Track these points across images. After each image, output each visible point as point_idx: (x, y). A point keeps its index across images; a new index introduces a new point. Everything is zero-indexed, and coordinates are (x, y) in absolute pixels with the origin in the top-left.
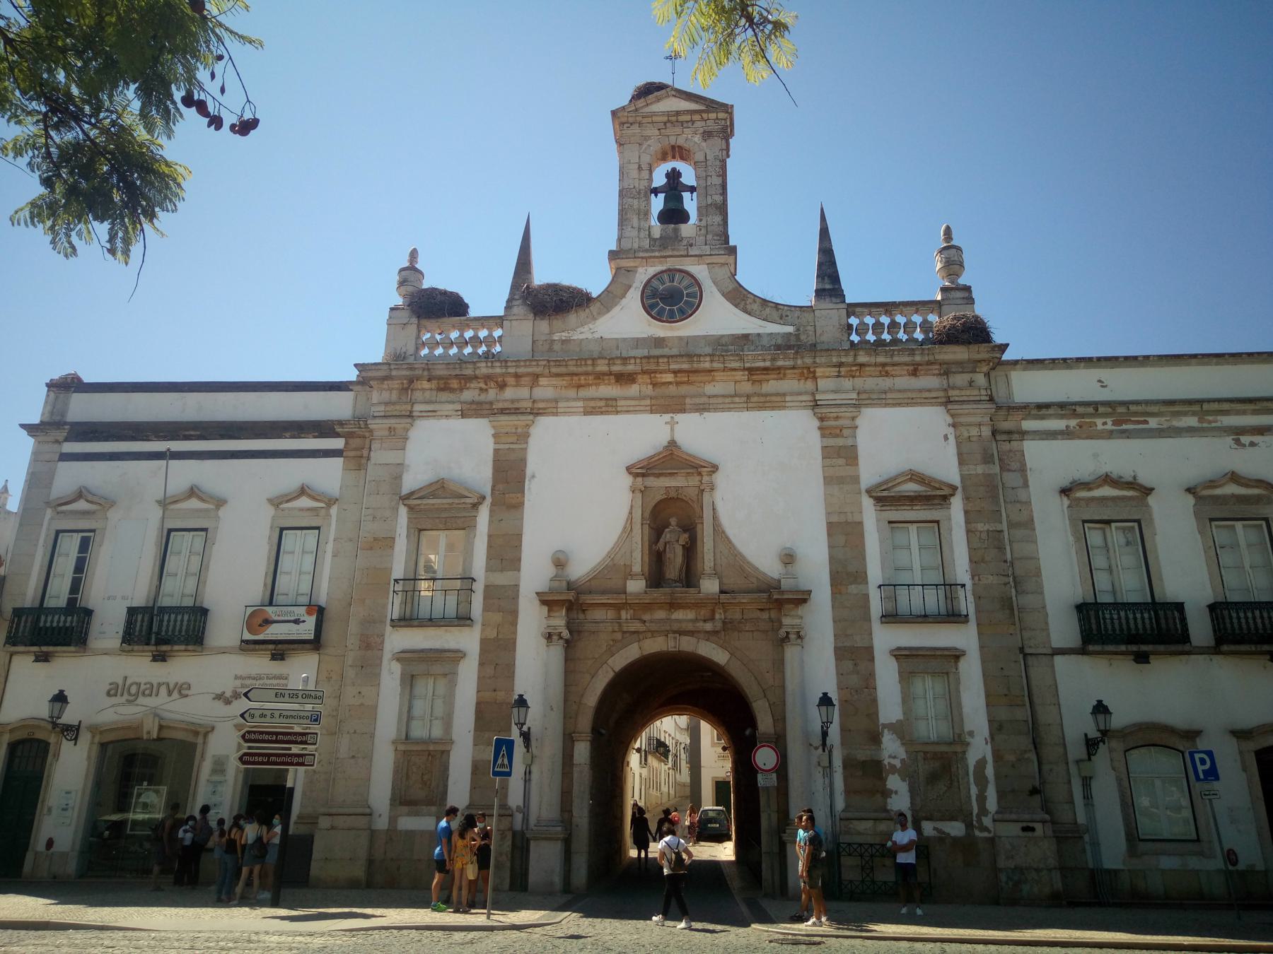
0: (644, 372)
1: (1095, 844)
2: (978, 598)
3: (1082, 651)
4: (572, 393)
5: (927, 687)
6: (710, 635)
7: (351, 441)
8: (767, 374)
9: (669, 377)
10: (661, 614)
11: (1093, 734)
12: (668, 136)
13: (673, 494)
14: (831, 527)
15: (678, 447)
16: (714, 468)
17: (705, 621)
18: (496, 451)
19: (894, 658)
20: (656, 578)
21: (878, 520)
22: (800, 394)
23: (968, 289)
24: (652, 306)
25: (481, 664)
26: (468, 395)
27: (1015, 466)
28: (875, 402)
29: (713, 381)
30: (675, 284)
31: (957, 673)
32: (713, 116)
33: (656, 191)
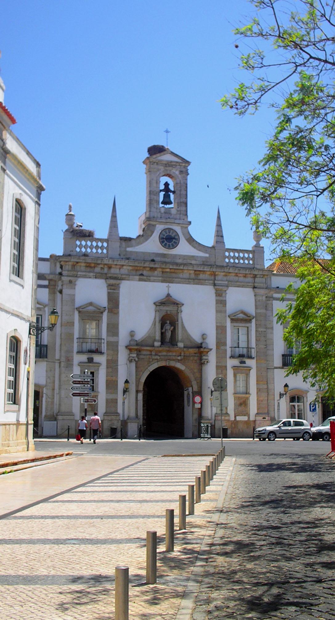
0: (160, 268)
2: (257, 352)
3: (282, 368)
4: (134, 272)
6: (179, 361)
7: (51, 282)
9: (168, 270)
11: (283, 392)
12: (167, 170)
13: (169, 313)
15: (171, 297)
17: (178, 356)
18: (109, 293)
19: (232, 370)
21: (231, 326)
23: (263, 247)
24: (166, 245)
25: (107, 368)
26: (98, 269)
27: (270, 309)
30: (171, 234)
32: (184, 165)
33: (161, 191)
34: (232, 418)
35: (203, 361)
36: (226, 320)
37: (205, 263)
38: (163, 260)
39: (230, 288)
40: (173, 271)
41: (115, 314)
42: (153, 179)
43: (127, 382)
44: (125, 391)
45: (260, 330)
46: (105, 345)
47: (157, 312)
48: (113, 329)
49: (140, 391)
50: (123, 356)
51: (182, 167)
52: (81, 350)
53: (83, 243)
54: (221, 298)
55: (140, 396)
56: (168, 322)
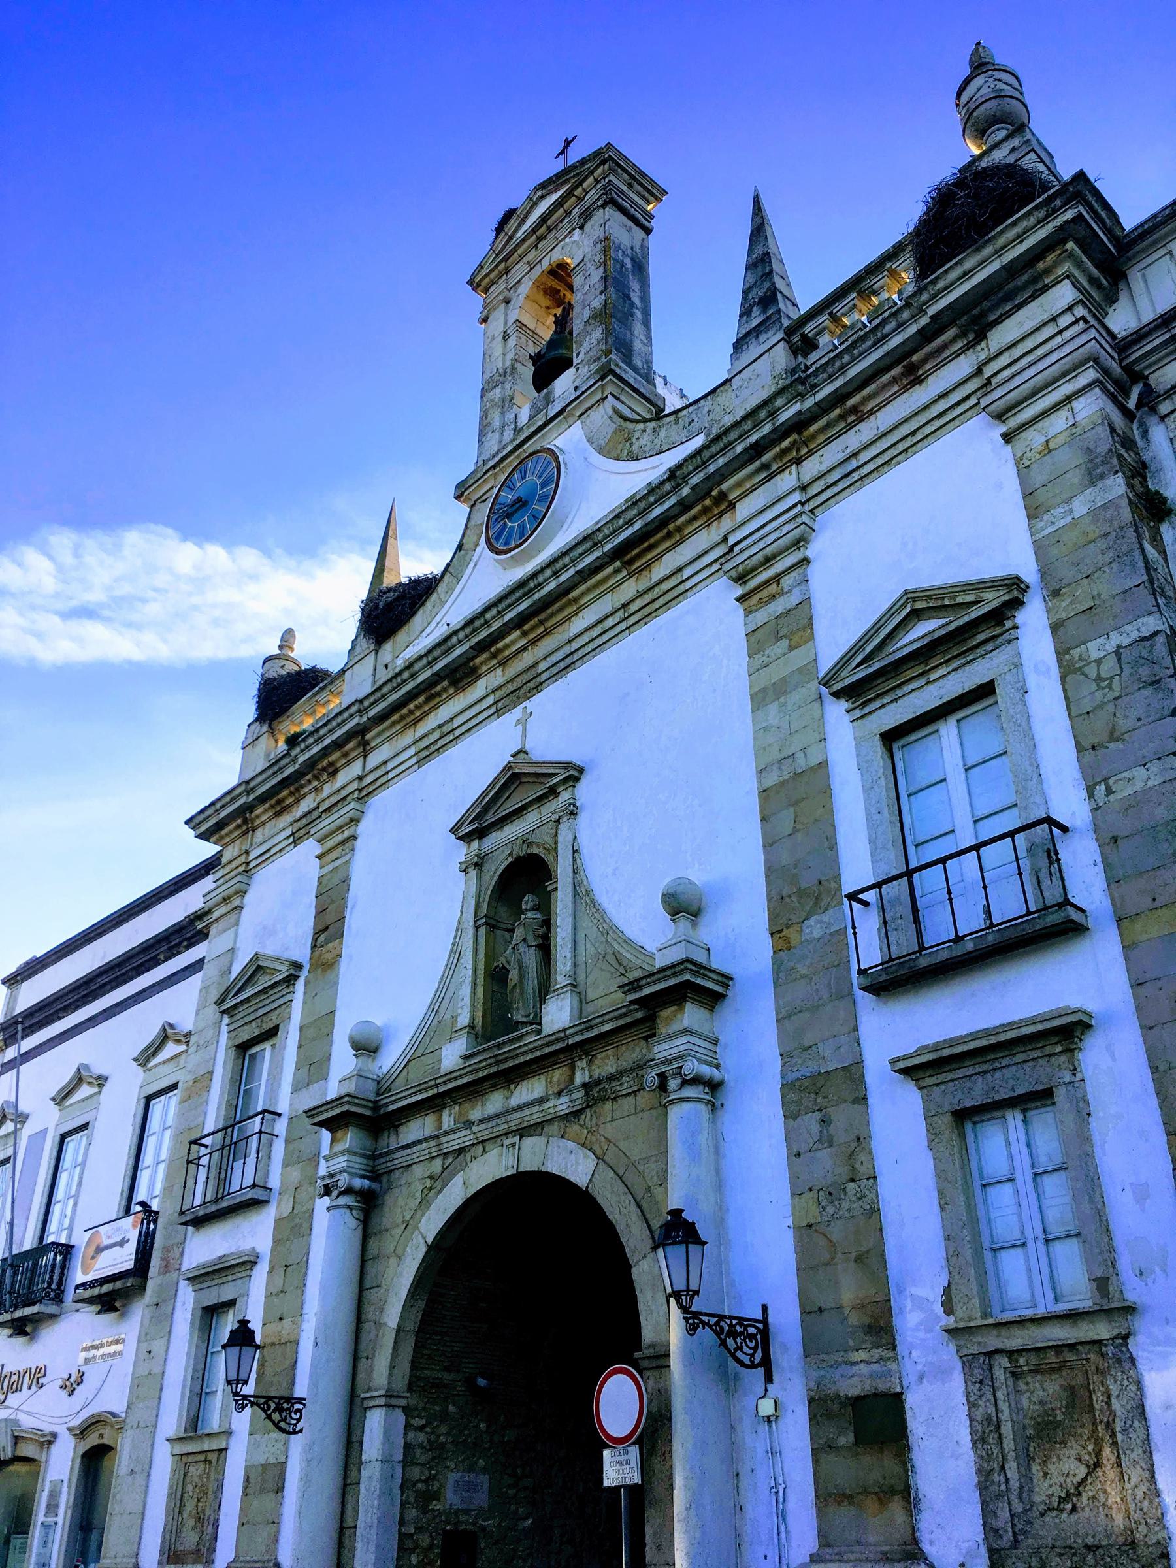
8: (651, 548)
10: (495, 1102)
13: (519, 851)
28: (841, 486)
29: (580, 609)
31: (1077, 1083)
45: (1095, 649)
47: (473, 873)
54: (778, 606)
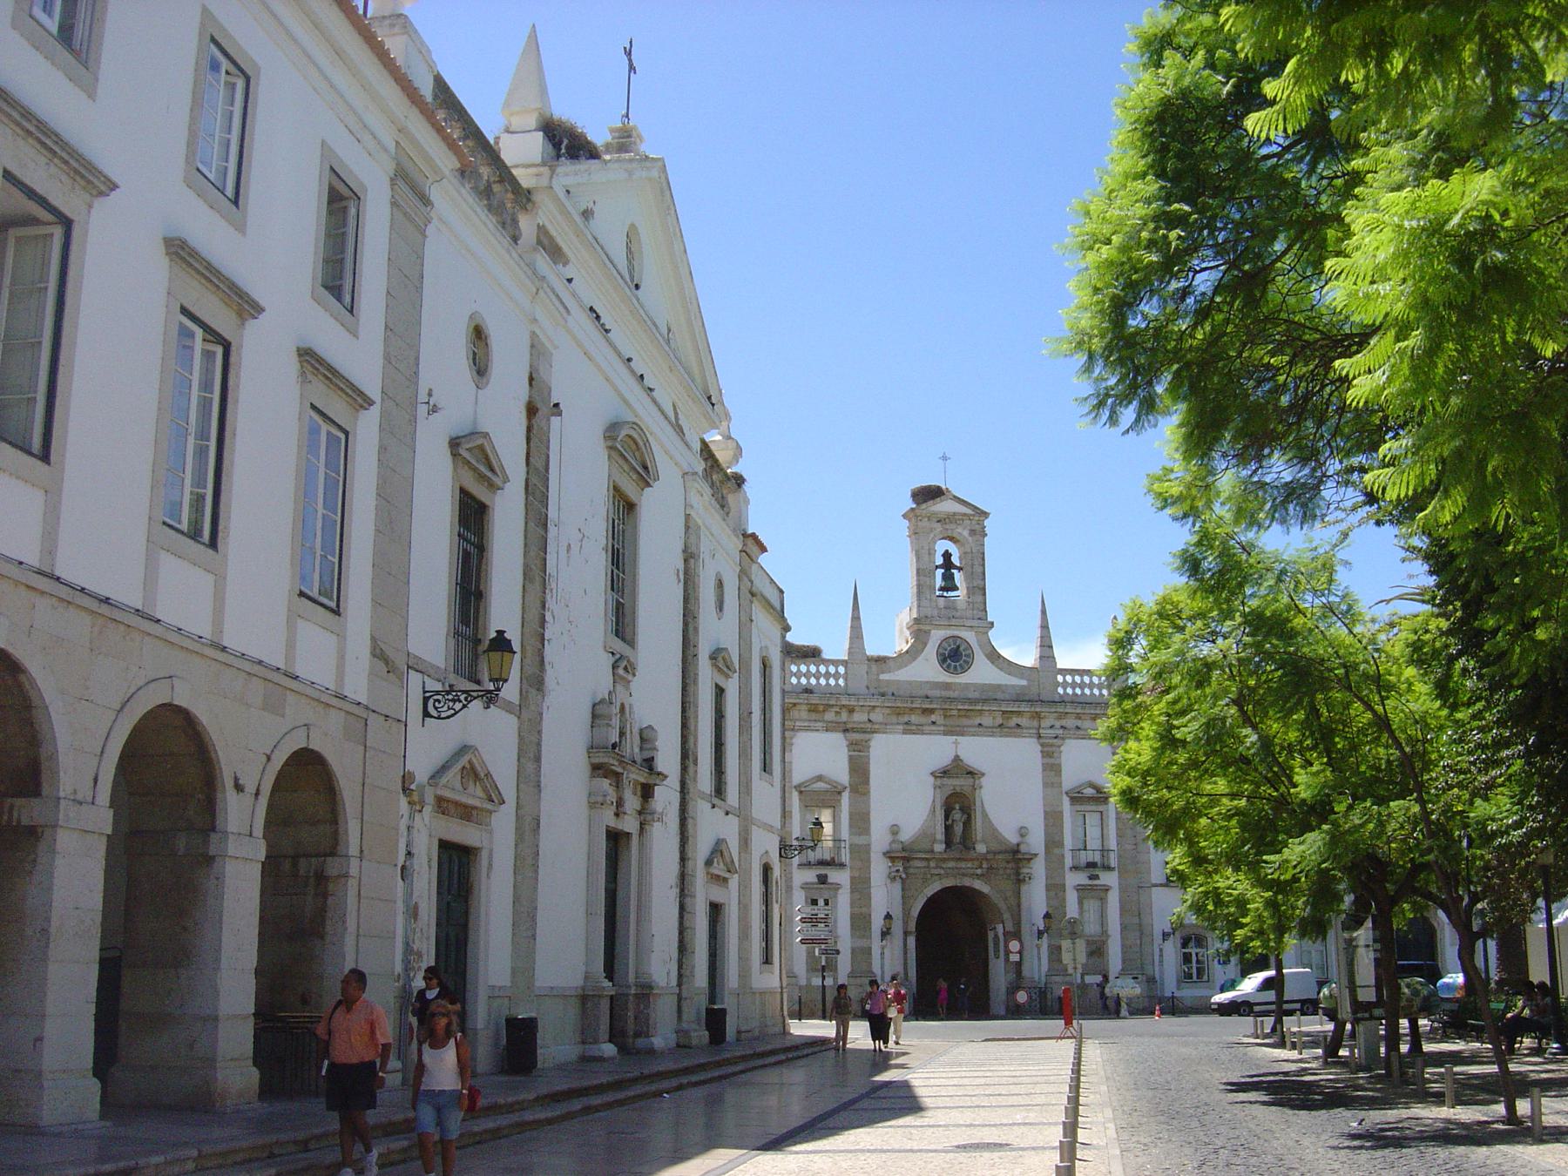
1: (1162, 984)
2: (1120, 857)
4: (894, 719)
5: (1092, 905)
9: (955, 712)
10: (951, 864)
13: (958, 789)
14: (1046, 813)
16: (983, 774)
18: (851, 758)
20: (949, 842)
22: (1030, 728)
24: (949, 666)
25: (852, 892)
26: (830, 716)
33: (937, 567)
34: (1079, 981)
35: (1021, 877)
36: (1061, 799)
37: (1020, 698)
38: (944, 693)
39: (1067, 741)
40: (962, 713)
41: (864, 794)
42: (922, 547)
43: (888, 917)
44: (885, 934)
46: (848, 850)
47: (938, 790)
48: (861, 821)
49: (911, 933)
50: (879, 869)
51: (974, 522)
52: (805, 861)
53: (803, 668)
54: (1051, 761)
55: (912, 941)
56: (957, 807)
